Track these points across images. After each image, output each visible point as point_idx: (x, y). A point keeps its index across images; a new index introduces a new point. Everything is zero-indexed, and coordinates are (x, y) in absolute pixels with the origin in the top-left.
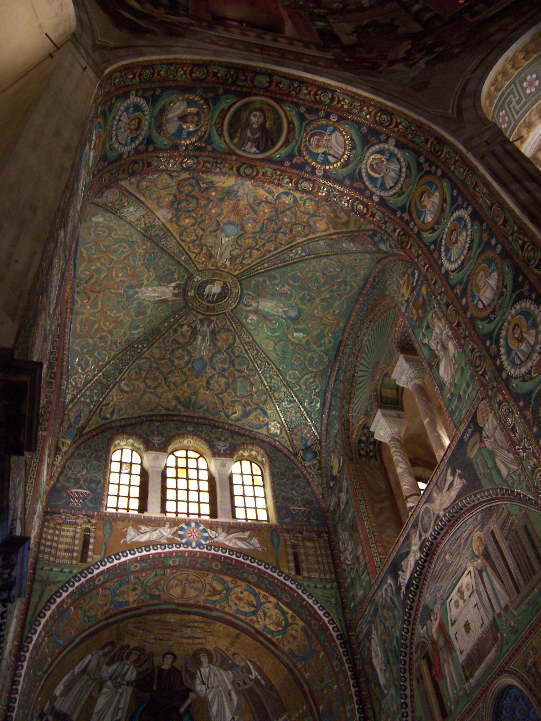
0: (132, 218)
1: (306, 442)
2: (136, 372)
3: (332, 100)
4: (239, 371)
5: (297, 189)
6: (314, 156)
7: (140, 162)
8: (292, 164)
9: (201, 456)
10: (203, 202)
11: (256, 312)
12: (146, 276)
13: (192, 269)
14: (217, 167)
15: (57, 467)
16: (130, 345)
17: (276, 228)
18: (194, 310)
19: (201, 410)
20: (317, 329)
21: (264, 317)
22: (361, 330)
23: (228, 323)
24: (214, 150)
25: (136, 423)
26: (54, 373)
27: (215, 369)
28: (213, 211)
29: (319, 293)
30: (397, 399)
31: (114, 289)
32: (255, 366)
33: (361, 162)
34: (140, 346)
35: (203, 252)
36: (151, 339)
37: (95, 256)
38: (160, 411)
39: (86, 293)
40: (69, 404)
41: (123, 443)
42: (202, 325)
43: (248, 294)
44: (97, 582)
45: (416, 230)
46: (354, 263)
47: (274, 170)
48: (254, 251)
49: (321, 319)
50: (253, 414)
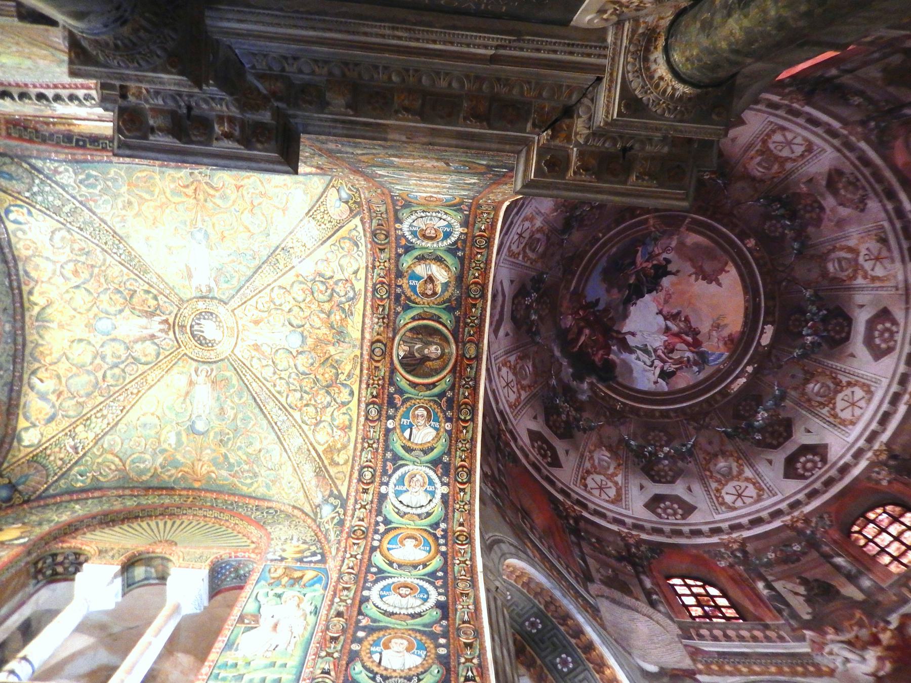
1: (24, 483)
2: (84, 249)
3: (465, 421)
4: (104, 376)
5: (367, 405)
6: (406, 415)
10: (327, 306)
13: (234, 303)
14: (379, 319)
17: (307, 389)
19: (36, 337)
20: (184, 457)
22: (201, 509)
23: (167, 353)
24: (397, 314)
27: (102, 346)
30: (133, 584)
31: (202, 216)
32: (114, 393)
33: (414, 463)
34: (121, 251)
36: (133, 263)
37: (245, 193)
38: (26, 284)
39: (192, 183)
40: (29, 164)
42: (160, 323)
43: (212, 370)
45: (376, 543)
47: (383, 378)
49: (200, 460)
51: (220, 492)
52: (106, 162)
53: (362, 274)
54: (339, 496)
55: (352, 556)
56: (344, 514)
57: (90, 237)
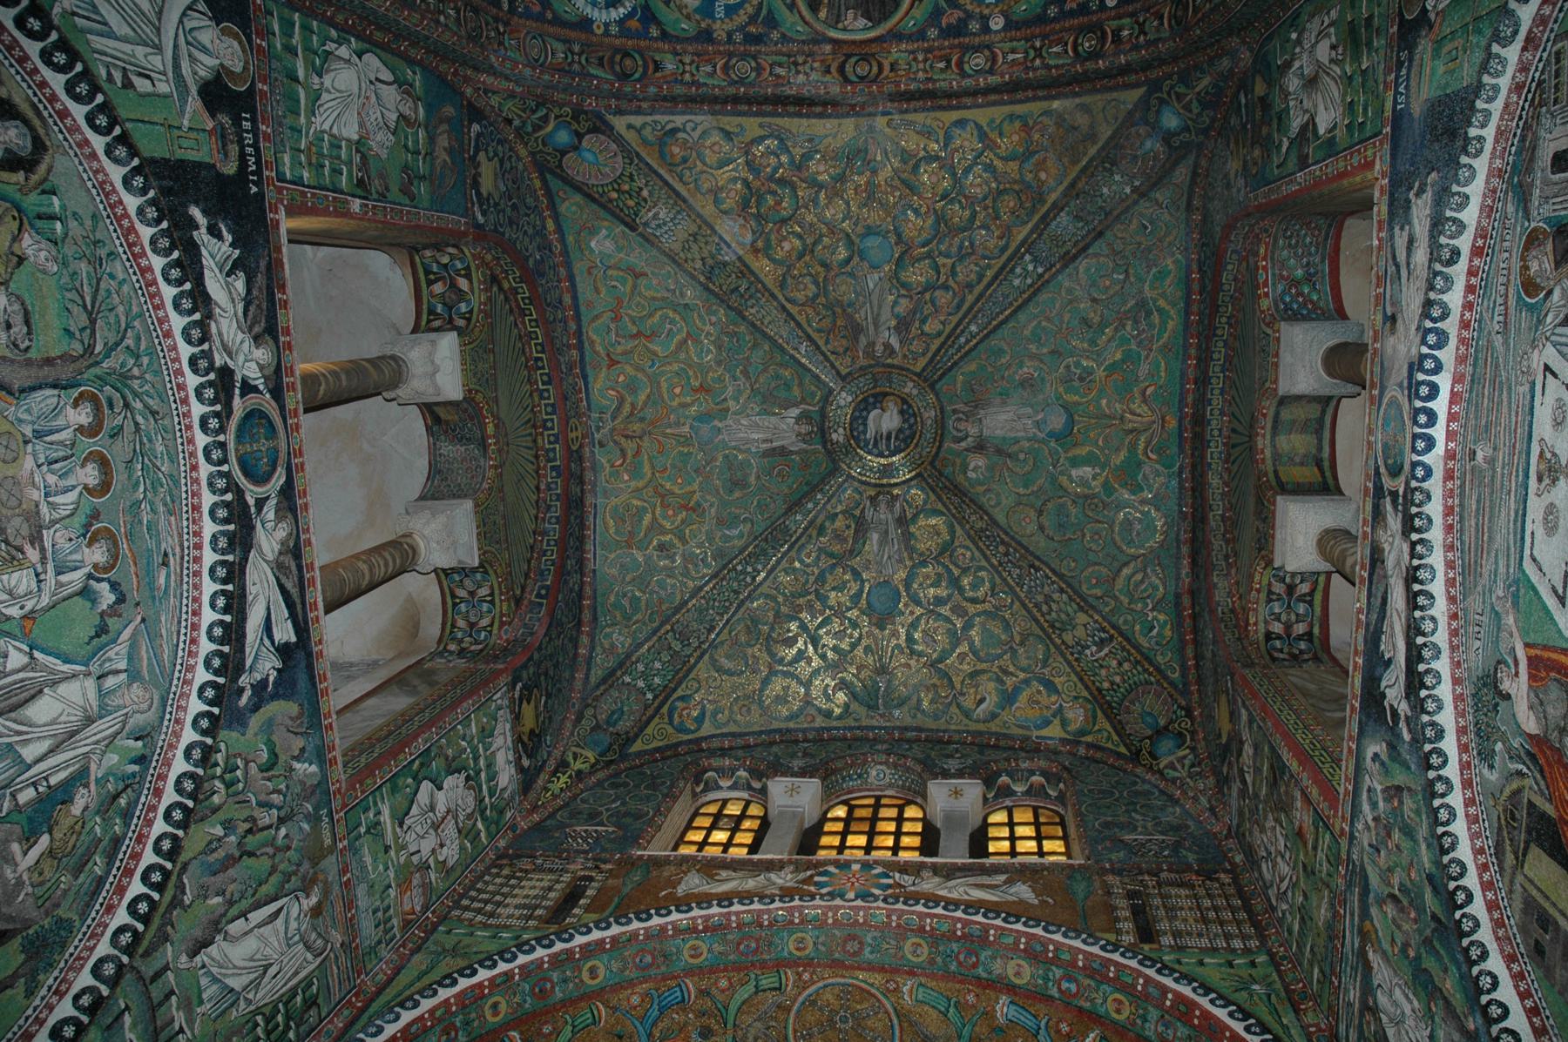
0: (671, 242)
4: (974, 601)
8: (941, 30)
9: (909, 802)
11: (980, 447)
12: (730, 391)
14: (798, 72)
15: (555, 797)
19: (906, 708)
20: (1118, 450)
21: (1000, 451)
25: (756, 745)
27: (918, 603)
30: (1325, 482)
34: (749, 569)
37: (619, 349)
38: (813, 720)
39: (616, 442)
40: (598, 687)
41: (725, 783)
43: (955, 411)
44: (585, 975)
48: (937, 293)
49: (1122, 418)
50: (1023, 697)
53: (730, 122)
54: (1144, 103)
56: (1170, 76)
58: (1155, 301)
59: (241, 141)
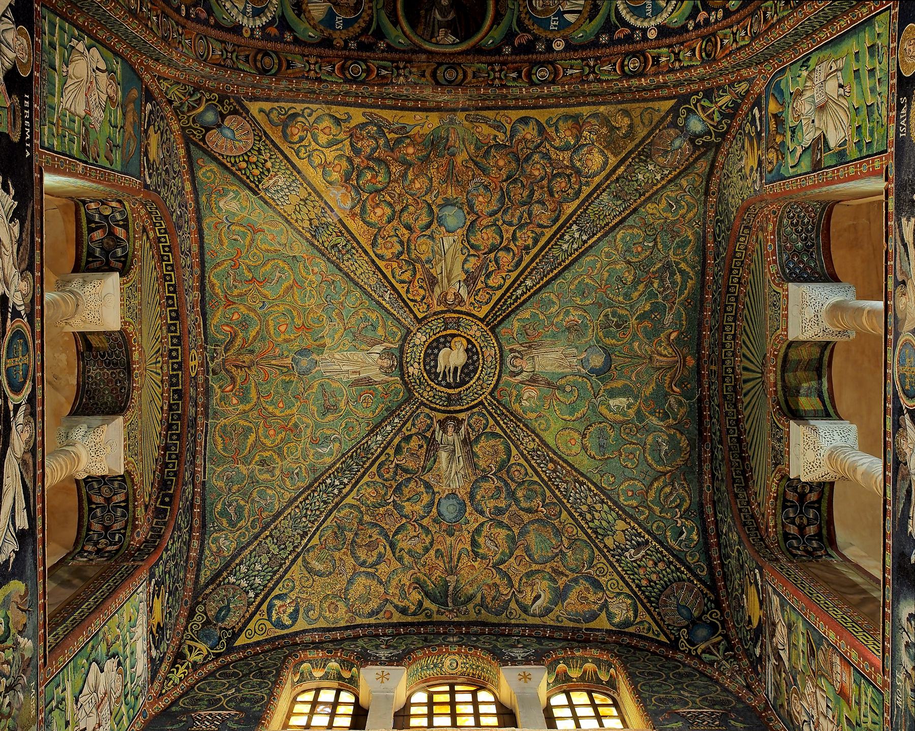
2: (336, 533)
4: (529, 511)
7: (274, 55)
11: (533, 380)
16: (317, 481)
17: (526, 193)
18: (425, 405)
23: (491, 422)
26: (171, 496)
27: (482, 513)
28: (418, 185)
29: (631, 307)
32: (556, 496)
34: (337, 483)
35: (418, 277)
39: (227, 371)
42: (445, 432)
43: (512, 351)
45: (720, 14)
46: (671, 218)
49: (651, 358)
51: (700, 325)
52: (204, 489)
55: (735, 40)
56: (697, 93)
57: (317, 524)
58: (677, 264)
59: (24, 114)
